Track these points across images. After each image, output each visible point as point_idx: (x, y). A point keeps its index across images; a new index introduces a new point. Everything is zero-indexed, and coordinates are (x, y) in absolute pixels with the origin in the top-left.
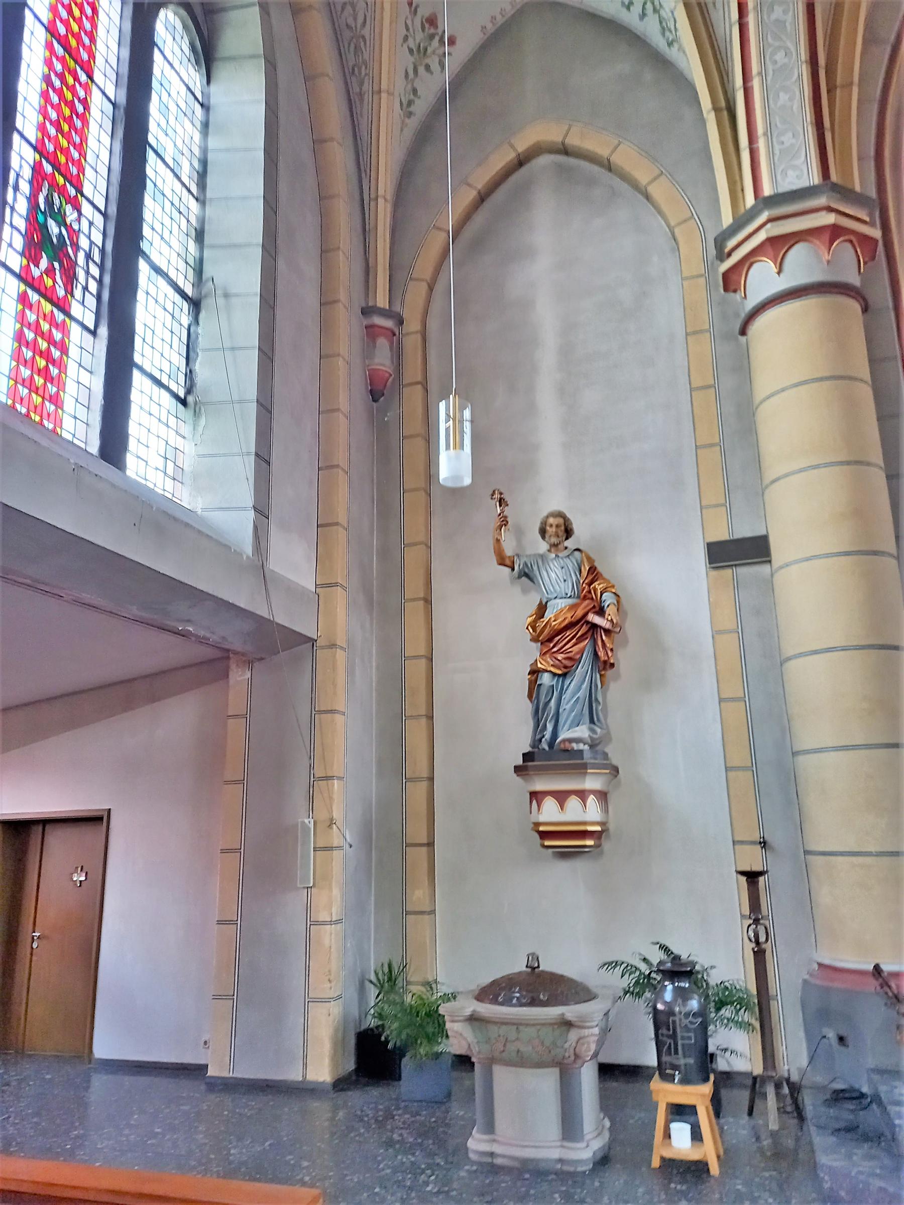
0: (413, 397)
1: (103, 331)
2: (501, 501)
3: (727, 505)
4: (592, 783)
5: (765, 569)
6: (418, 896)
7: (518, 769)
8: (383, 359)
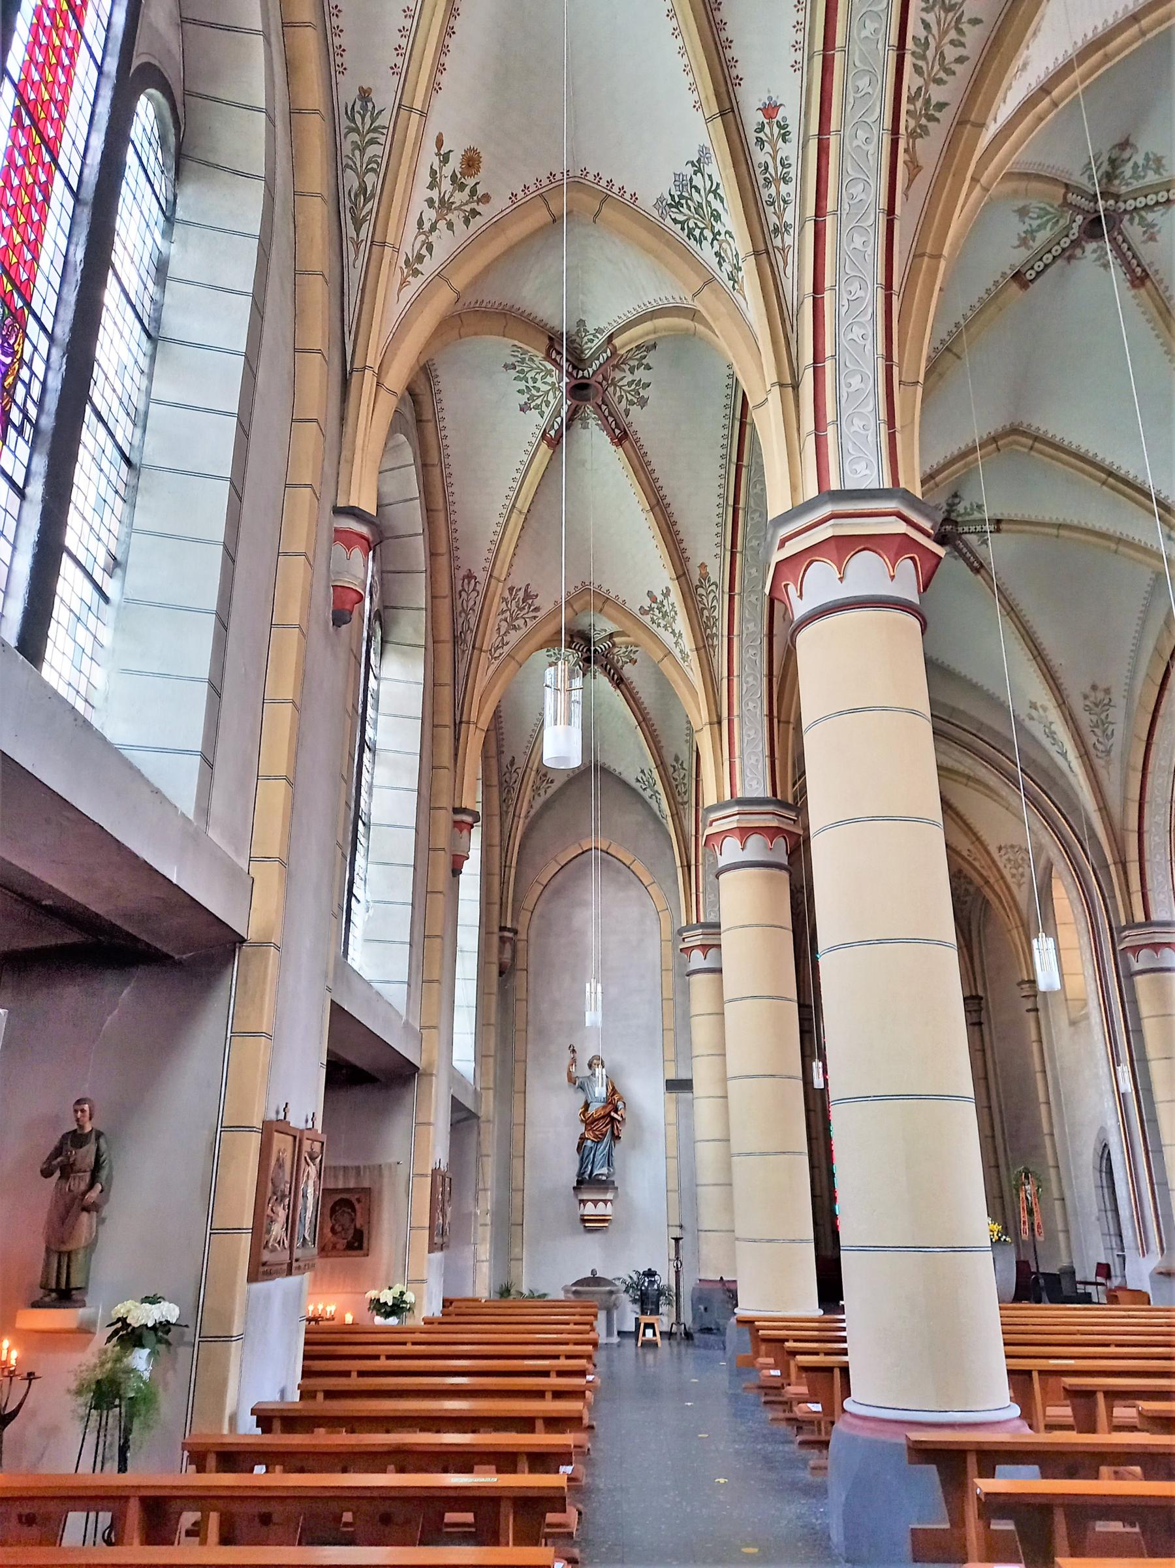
2: (574, 1051)
3: (676, 1061)
4: (609, 1196)
5: (689, 1095)
6: (517, 1250)
7: (574, 1188)
8: (507, 955)
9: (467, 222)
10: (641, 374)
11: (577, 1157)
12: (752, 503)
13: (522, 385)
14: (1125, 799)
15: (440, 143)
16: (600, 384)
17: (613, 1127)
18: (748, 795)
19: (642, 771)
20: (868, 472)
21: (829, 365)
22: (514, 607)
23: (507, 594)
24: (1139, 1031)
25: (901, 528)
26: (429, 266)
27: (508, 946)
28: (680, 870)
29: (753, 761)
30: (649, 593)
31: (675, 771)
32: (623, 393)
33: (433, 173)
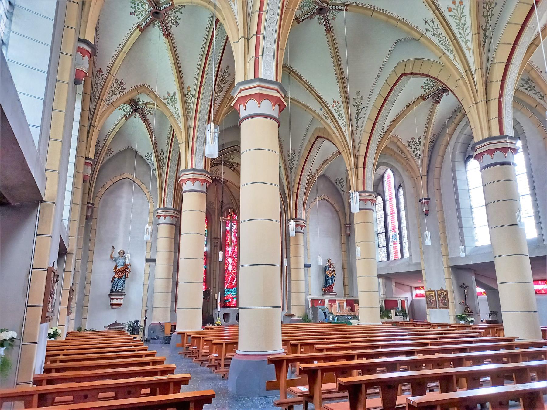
0: (94, 221)
2: (114, 248)
4: (122, 297)
5: (154, 264)
7: (109, 294)
8: (90, 213)
10: (178, 14)
11: (111, 284)
12: (209, 70)
13: (133, 5)
14: (294, 183)
16: (164, 14)
17: (126, 274)
18: (197, 168)
19: (148, 153)
20: (270, 74)
21: (261, 36)
22: (116, 87)
23: (114, 81)
24: (289, 249)
25: (278, 95)
27: (90, 209)
28: (158, 190)
29: (199, 157)
30: (168, 93)
31: (161, 155)
32: (171, 20)
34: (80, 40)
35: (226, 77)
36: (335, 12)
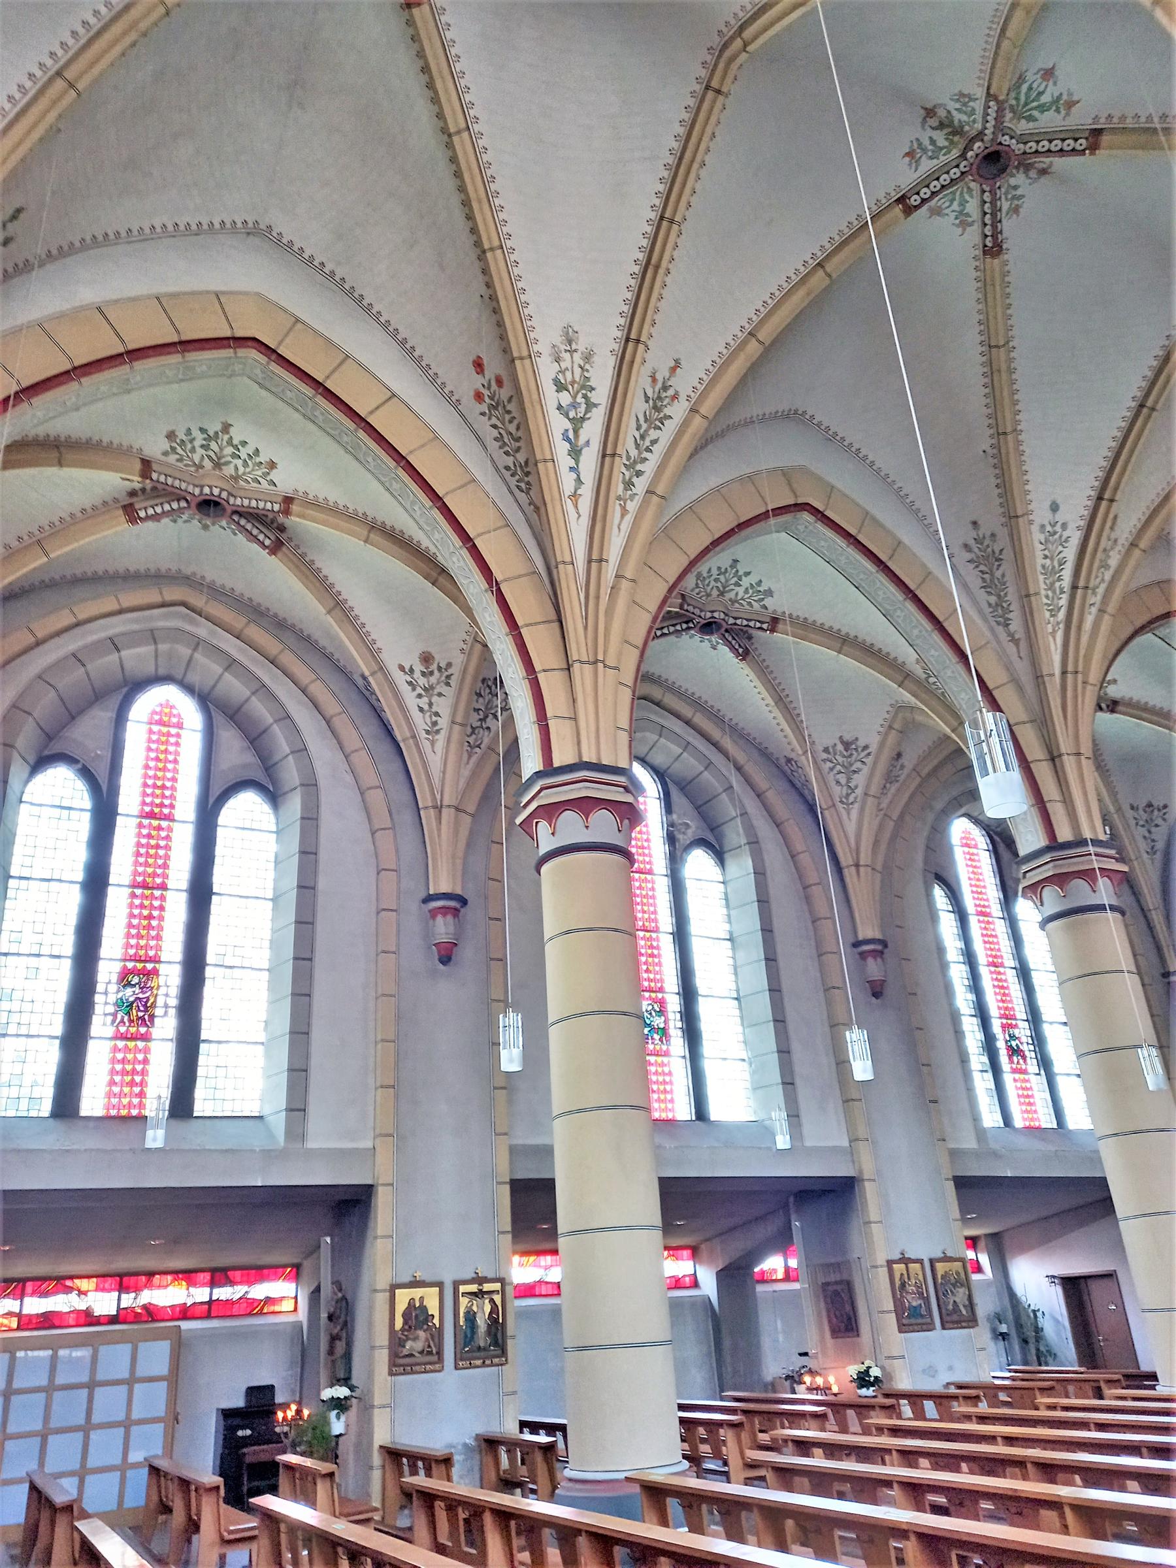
1: (1042, 1072)
9: (448, 684)
10: (746, 582)
15: (402, 668)
22: (840, 759)
23: (825, 756)
26: (443, 722)
33: (410, 683)
34: (429, 898)
35: (989, 550)
36: (1046, 99)
